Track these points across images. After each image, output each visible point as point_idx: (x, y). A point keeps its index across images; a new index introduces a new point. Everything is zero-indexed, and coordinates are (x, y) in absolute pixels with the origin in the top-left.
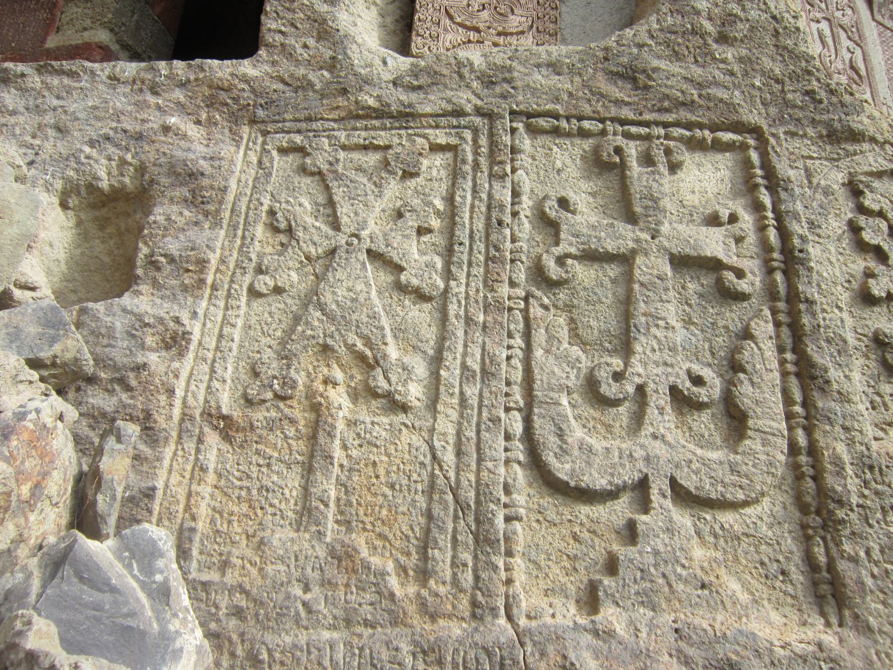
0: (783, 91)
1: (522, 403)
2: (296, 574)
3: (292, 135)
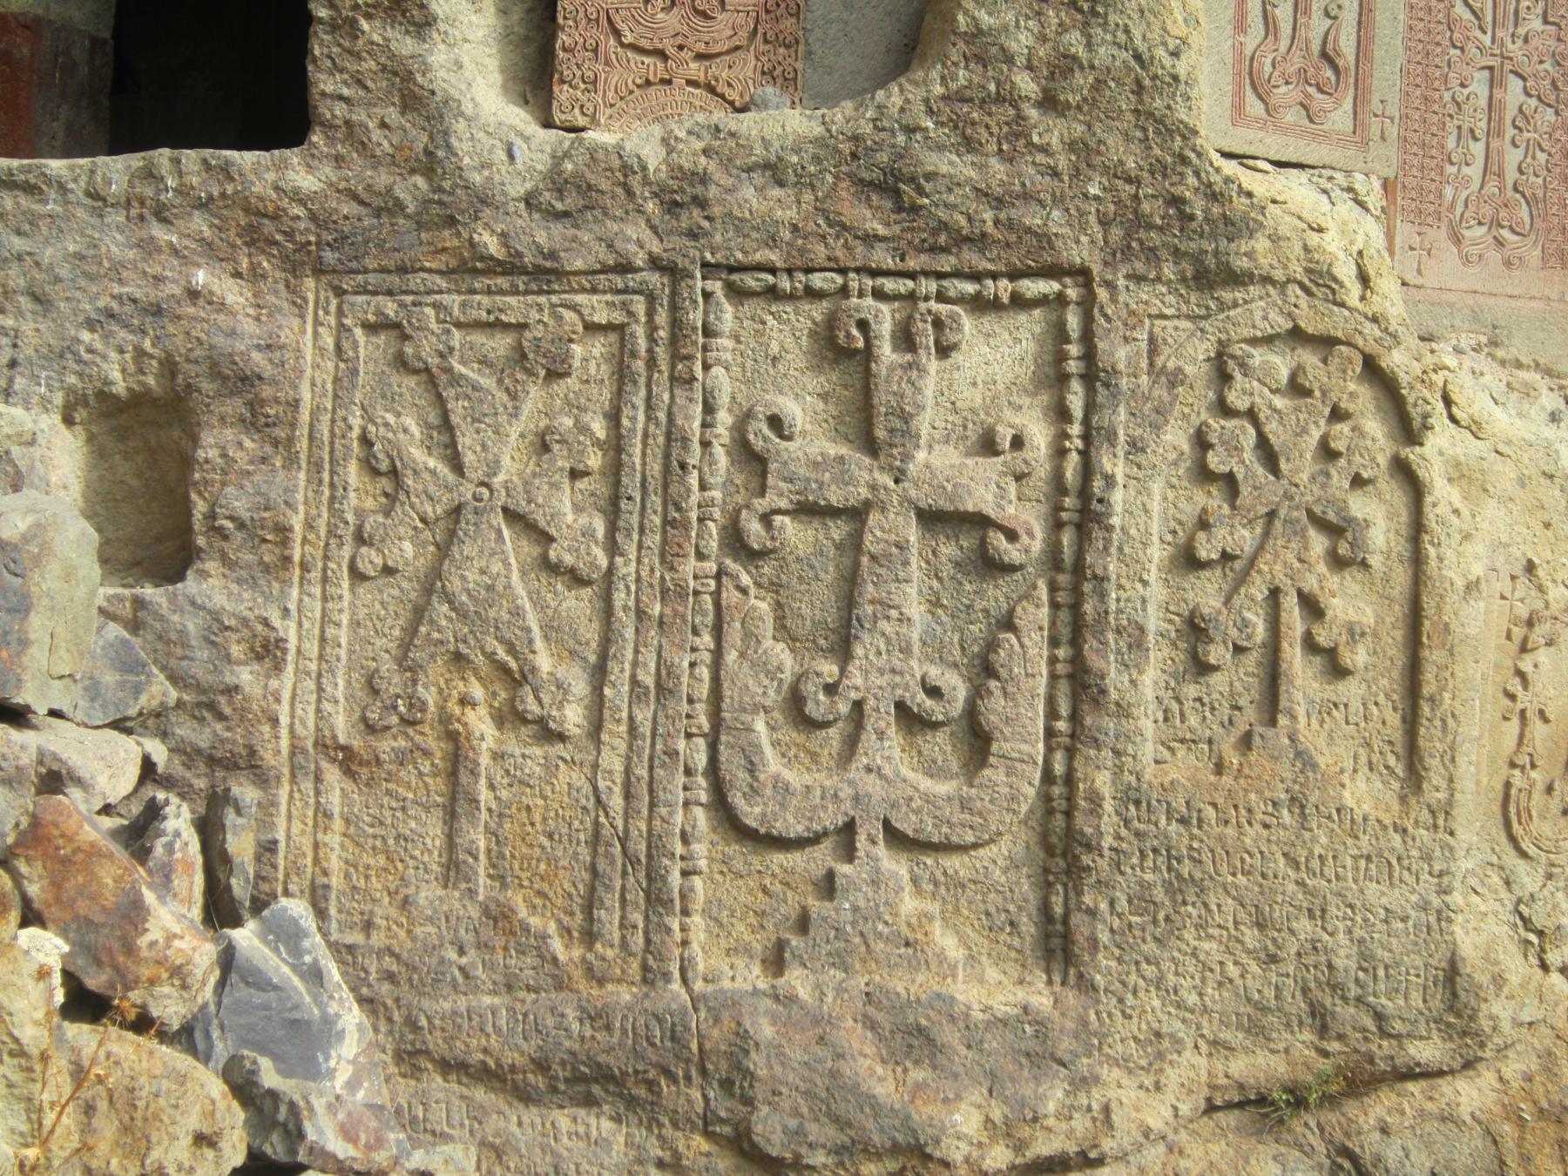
0: (1136, 197)
1: (706, 727)
2: (448, 937)
3: (380, 297)
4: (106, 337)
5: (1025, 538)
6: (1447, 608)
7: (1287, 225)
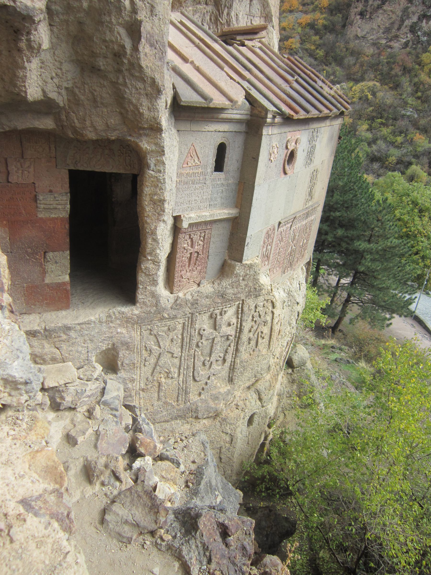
4: (103, 343)
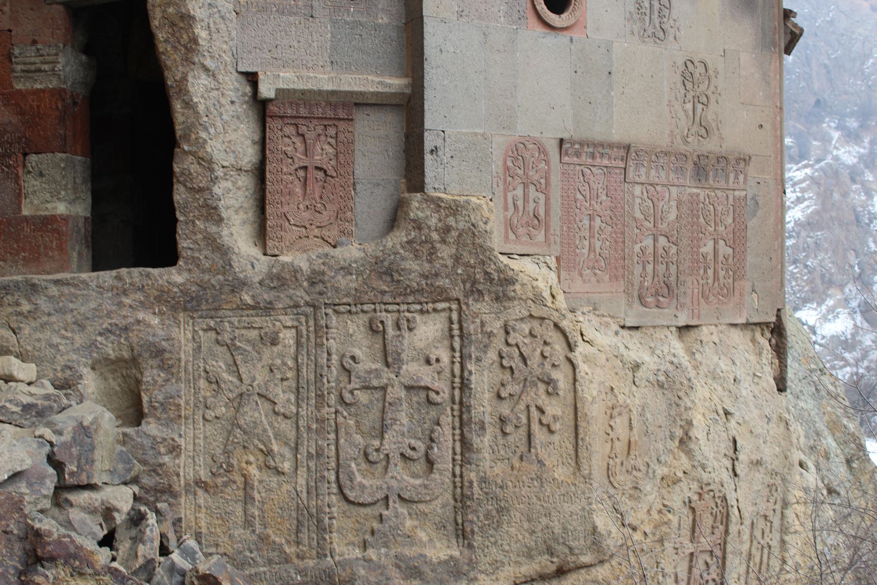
4: (107, 339)
5: (442, 394)
6: (586, 408)
7: (526, 279)
